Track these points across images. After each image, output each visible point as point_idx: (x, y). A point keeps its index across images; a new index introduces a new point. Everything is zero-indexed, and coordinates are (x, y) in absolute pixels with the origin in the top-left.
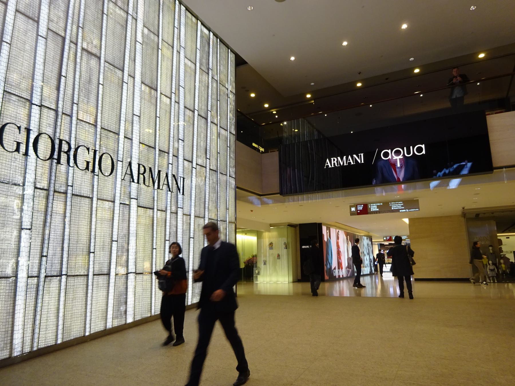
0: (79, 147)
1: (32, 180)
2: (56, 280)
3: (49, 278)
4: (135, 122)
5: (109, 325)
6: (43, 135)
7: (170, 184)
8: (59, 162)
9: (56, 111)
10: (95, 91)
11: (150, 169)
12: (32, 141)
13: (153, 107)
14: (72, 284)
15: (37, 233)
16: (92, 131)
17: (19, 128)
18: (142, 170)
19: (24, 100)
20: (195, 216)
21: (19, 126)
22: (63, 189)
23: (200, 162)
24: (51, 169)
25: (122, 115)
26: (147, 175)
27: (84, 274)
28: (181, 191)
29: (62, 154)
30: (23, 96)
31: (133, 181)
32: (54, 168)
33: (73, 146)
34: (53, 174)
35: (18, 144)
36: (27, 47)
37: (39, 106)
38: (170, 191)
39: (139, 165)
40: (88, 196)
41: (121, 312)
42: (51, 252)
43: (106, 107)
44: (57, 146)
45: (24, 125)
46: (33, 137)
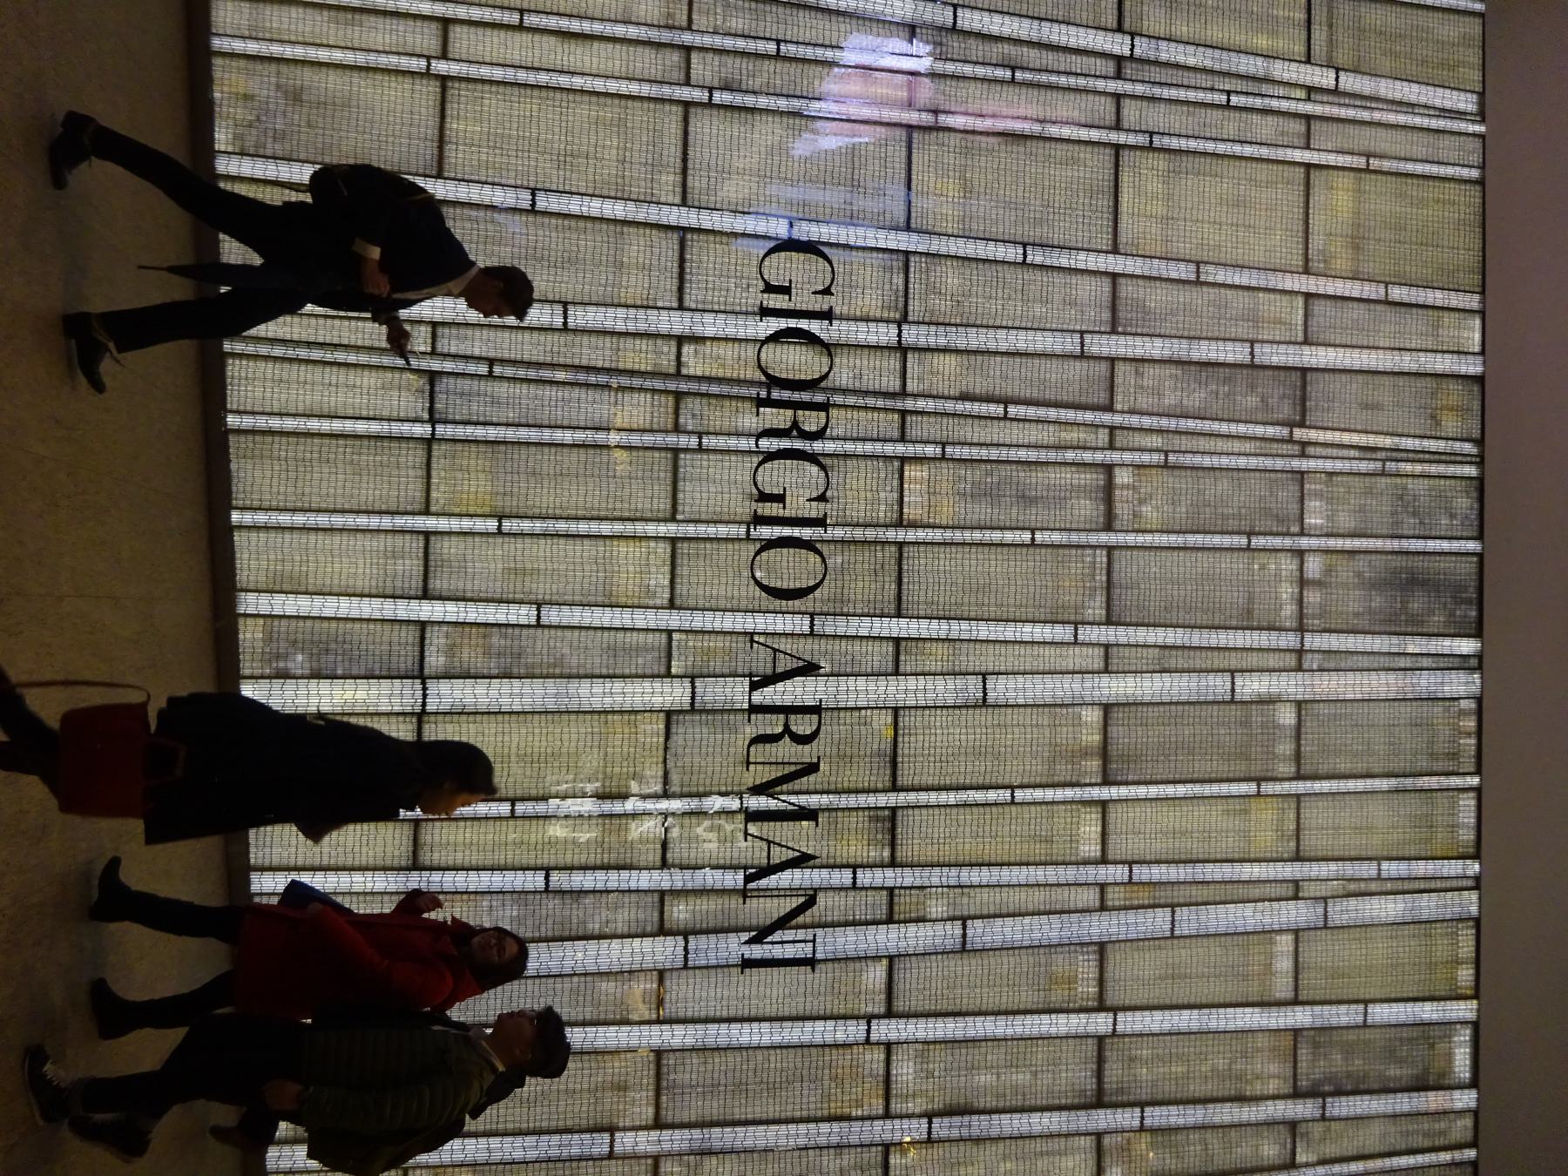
0: (823, 467)
1: (699, 330)
2: (420, 407)
3: (427, 387)
4: (960, 681)
5: (249, 603)
6: (825, 360)
7: (772, 881)
8: (761, 403)
9: (903, 393)
10: (1003, 519)
11: (812, 768)
12: (803, 324)
13: (1038, 769)
14: (403, 460)
15: (555, 349)
16: (882, 515)
17: (827, 291)
18: (803, 726)
19: (901, 305)
20: (659, 1053)
21: (833, 290)
22: (687, 421)
23: (905, 1070)
24: (739, 382)
25: (965, 625)
26: (786, 750)
27: (433, 502)
28: (757, 952)
29: (789, 413)
30: (911, 302)
31: (754, 687)
32: (744, 391)
33: (818, 446)
34: (725, 389)
35: (786, 290)
36: (1038, 310)
37: (899, 342)
38: (748, 879)
39: (816, 710)
40: (680, 508)
41: (286, 657)
42: (502, 389)
43: (974, 563)
44: (805, 396)
45: (836, 303)
46: (814, 326)
